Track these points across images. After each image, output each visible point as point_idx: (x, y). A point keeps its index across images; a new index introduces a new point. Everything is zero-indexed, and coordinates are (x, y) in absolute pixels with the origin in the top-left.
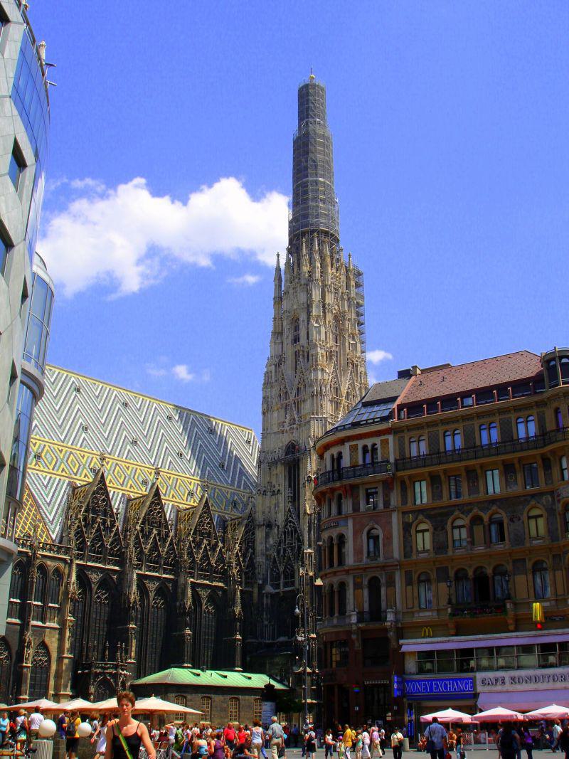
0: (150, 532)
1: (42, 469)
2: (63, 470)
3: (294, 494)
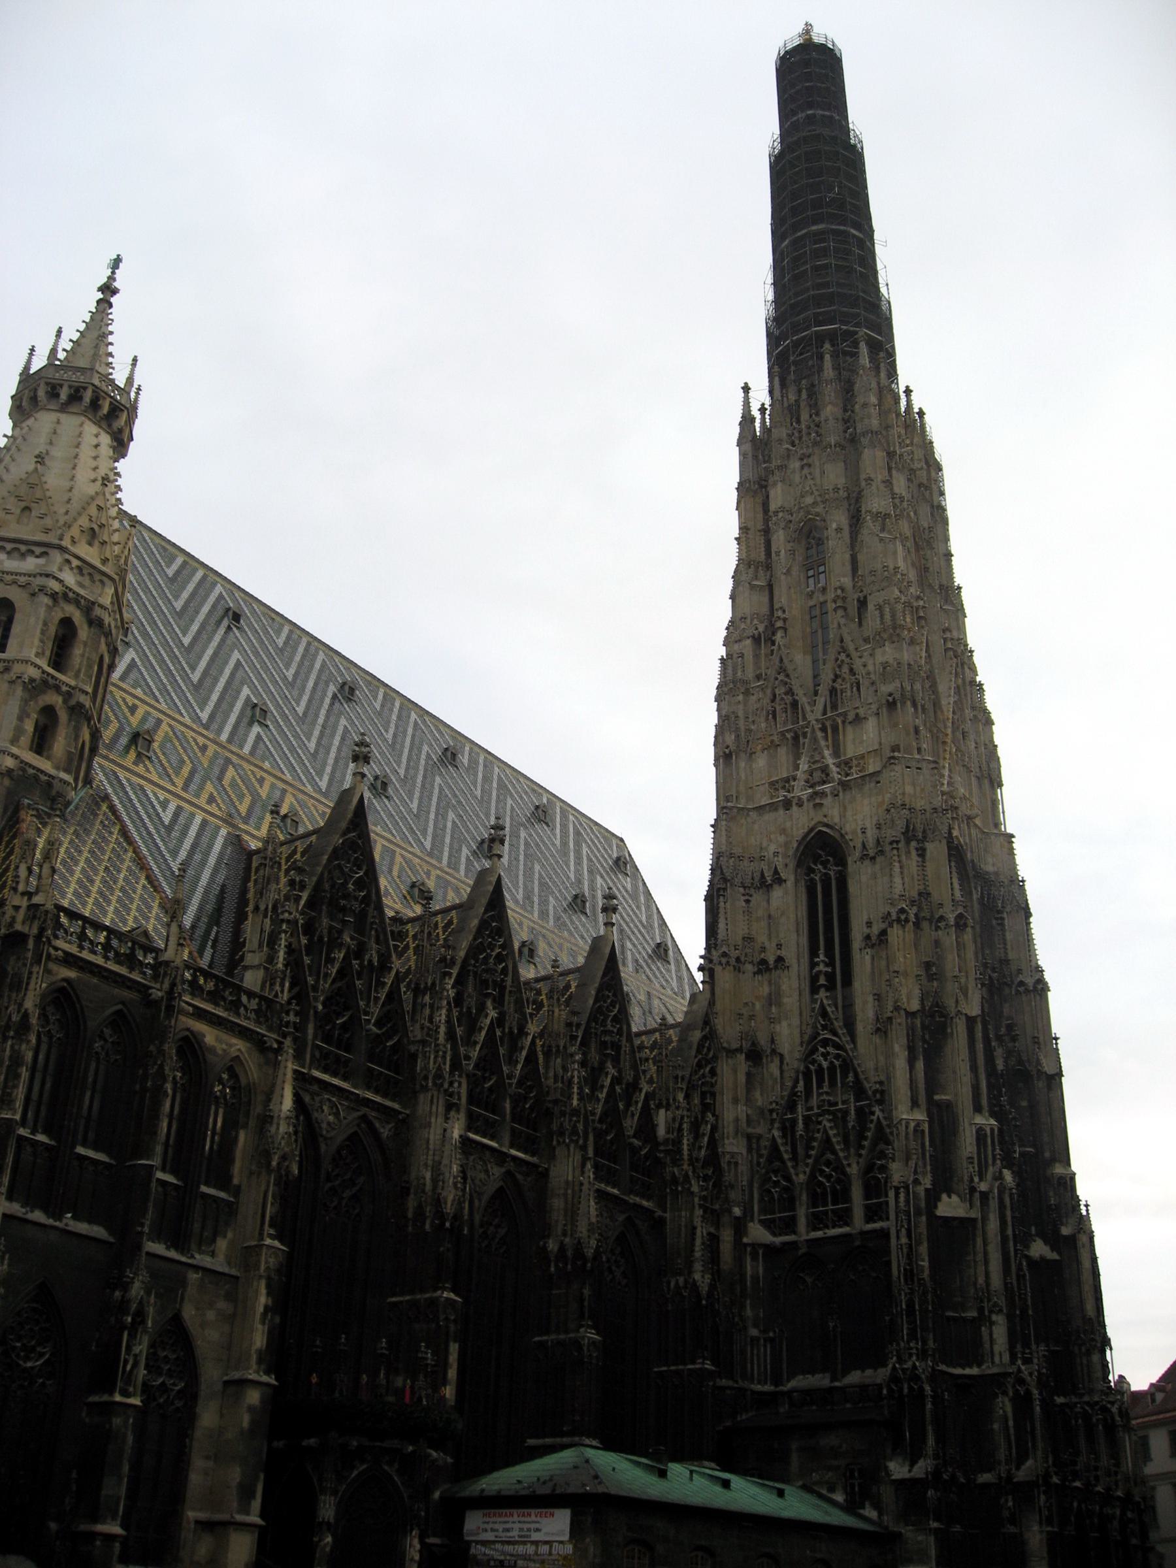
0: (482, 1008)
1: (155, 778)
2: (211, 800)
3: (831, 963)
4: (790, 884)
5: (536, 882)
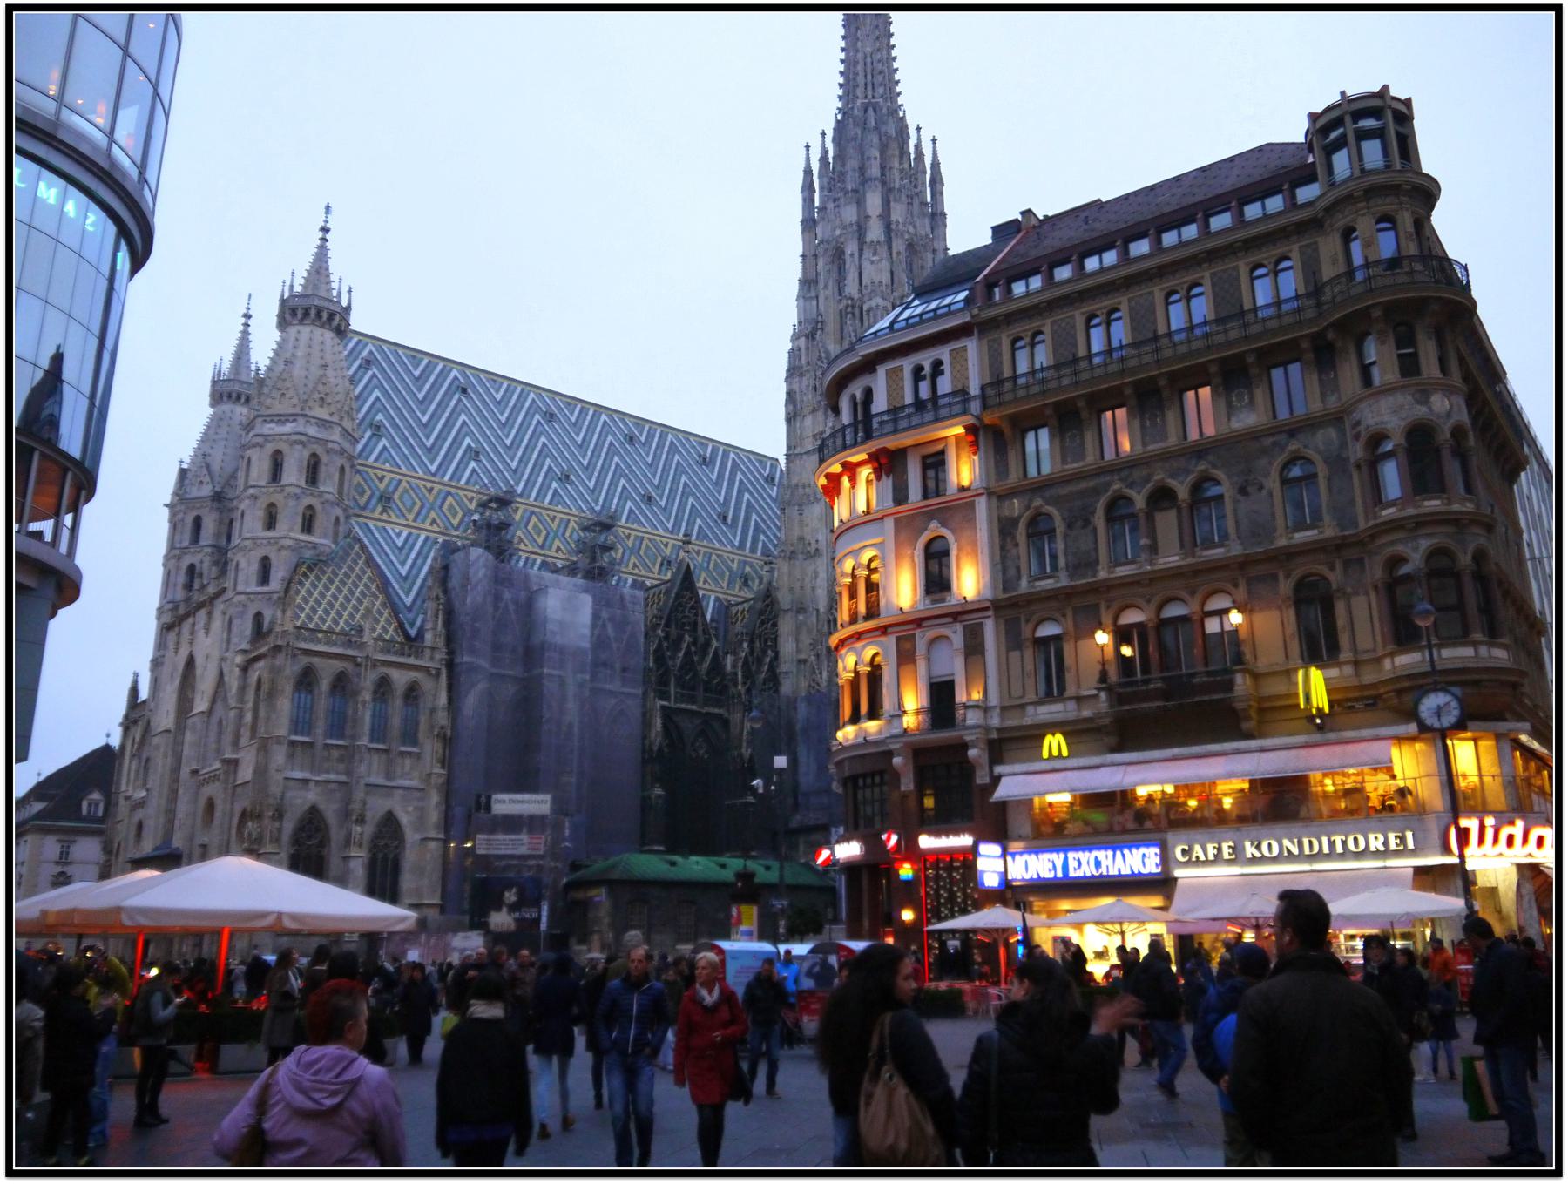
1: (394, 519)
2: (434, 522)
4: (822, 502)
5: (687, 511)
